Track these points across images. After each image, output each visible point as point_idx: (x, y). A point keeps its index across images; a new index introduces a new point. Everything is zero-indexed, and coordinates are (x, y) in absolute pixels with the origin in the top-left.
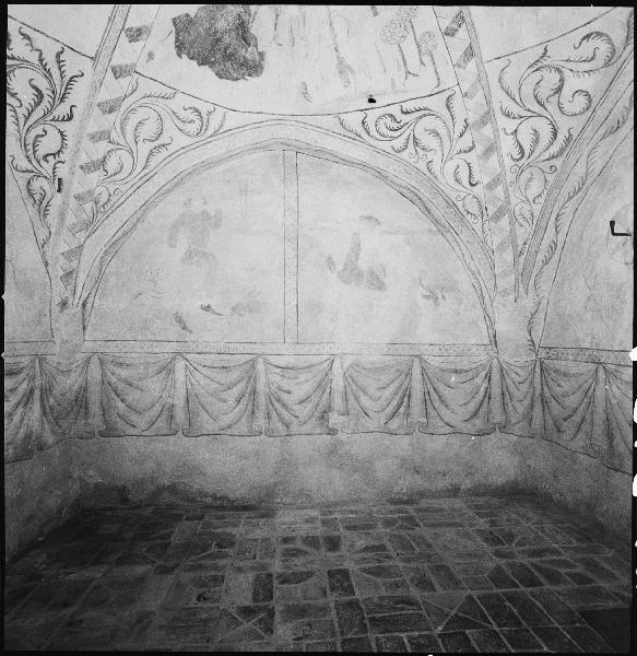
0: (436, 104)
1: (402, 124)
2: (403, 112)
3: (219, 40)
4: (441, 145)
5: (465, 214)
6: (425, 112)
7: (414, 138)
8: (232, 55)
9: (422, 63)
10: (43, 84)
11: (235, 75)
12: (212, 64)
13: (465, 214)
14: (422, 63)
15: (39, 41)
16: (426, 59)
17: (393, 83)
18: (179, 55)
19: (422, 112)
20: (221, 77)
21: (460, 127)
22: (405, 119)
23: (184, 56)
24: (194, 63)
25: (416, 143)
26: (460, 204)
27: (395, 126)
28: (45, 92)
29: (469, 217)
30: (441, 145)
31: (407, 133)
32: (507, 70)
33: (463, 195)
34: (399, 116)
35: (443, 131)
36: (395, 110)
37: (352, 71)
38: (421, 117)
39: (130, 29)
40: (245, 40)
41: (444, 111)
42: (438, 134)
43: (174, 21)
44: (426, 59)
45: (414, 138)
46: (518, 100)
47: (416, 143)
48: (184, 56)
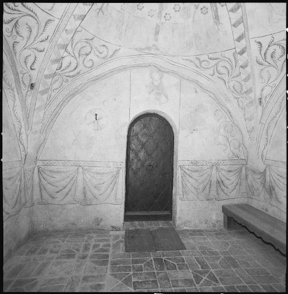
1: (16, 8)
4: (29, 38)
5: (21, 82)
7: (17, 21)
13: (21, 82)
19: (32, 14)
21: (44, 37)
25: (15, 25)
26: (20, 76)
29: (22, 85)
30: (29, 38)
31: (14, 16)
33: (24, 71)
38: (30, 15)
41: (43, 24)
45: (17, 21)
46: (73, 48)
47: (15, 25)
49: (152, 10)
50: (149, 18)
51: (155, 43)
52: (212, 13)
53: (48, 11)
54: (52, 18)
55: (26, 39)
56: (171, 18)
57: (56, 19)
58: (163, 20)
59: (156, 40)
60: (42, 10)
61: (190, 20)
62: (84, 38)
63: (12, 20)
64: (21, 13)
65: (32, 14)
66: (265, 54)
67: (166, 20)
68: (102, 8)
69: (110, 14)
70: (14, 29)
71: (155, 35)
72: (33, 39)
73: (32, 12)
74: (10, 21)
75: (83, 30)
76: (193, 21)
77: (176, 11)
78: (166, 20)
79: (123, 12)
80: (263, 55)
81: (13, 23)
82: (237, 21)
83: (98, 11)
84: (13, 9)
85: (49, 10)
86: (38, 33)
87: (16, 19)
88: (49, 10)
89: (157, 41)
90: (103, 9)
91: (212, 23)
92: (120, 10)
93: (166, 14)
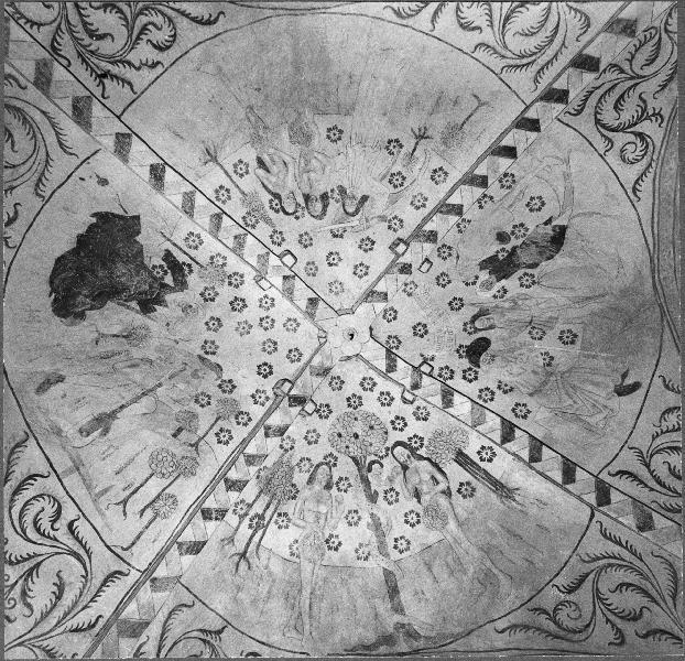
0: (102, 562)
1: (52, 533)
2: (70, 525)
3: (104, 264)
4: (45, 616)
6: (82, 555)
7: (39, 564)
8: (82, 277)
9: (143, 511)
10: (106, 47)
11: (57, 282)
12: (74, 252)
14: (143, 511)
15: (148, 75)
16: (149, 514)
17: (106, 490)
18: (94, 215)
19: (82, 552)
20: (58, 260)
21: (83, 618)
22: (62, 534)
23: (94, 220)
24: (82, 230)
27: (45, 525)
28: (95, 45)
30: (45, 616)
32: (184, 609)
34: (62, 524)
35: (69, 597)
36: (70, 513)
37: (106, 431)
39: (163, 171)
40: (100, 294)
41: (97, 582)
42: (59, 598)
43: (137, 218)
44: (149, 514)
45: (39, 564)
48: (94, 220)
49: (361, 545)
50: (360, 563)
51: (397, 618)
52: (483, 483)
53: (119, 551)
54: (124, 568)
55: (37, 615)
56: (409, 543)
57: (133, 571)
58: (395, 555)
59: (399, 609)
60: (108, 547)
61: (452, 525)
62: (200, 626)
63: (30, 557)
64: (55, 544)
65: (82, 552)
66: (659, 482)
67: (401, 552)
68: (245, 552)
69: (266, 567)
70: (20, 582)
71: (392, 598)
72: (55, 622)
73: (84, 547)
74: (25, 560)
75: (198, 604)
76: (460, 524)
77: (413, 525)
78: (401, 552)
79: (298, 560)
80: (658, 487)
81: (27, 565)
82: (530, 451)
83: (236, 558)
84: (43, 535)
85: (124, 549)
86: (75, 604)
87: (40, 559)
88: (124, 549)
89: (402, 610)
90: (248, 555)
91: (498, 503)
92: (287, 556)
93: (396, 540)
